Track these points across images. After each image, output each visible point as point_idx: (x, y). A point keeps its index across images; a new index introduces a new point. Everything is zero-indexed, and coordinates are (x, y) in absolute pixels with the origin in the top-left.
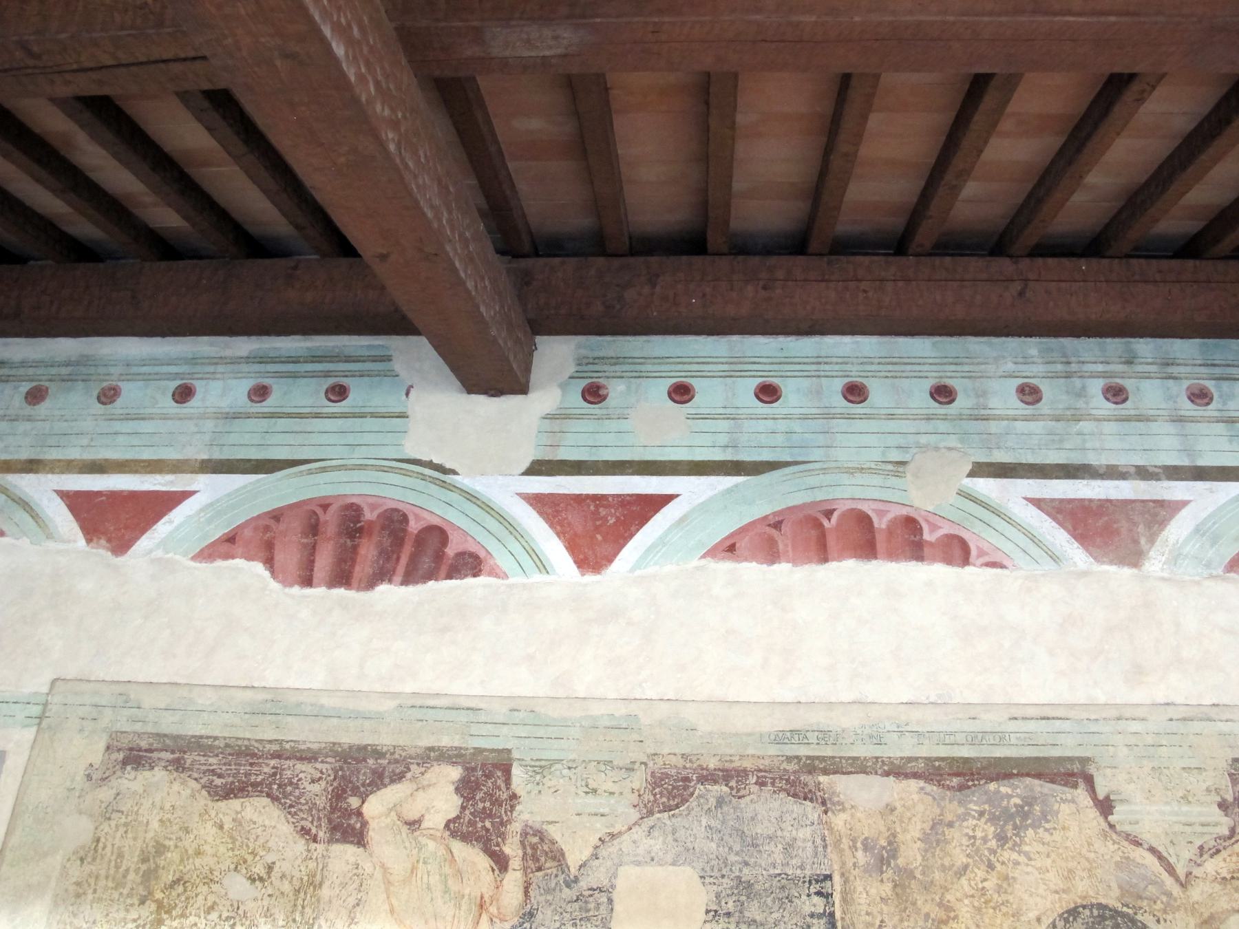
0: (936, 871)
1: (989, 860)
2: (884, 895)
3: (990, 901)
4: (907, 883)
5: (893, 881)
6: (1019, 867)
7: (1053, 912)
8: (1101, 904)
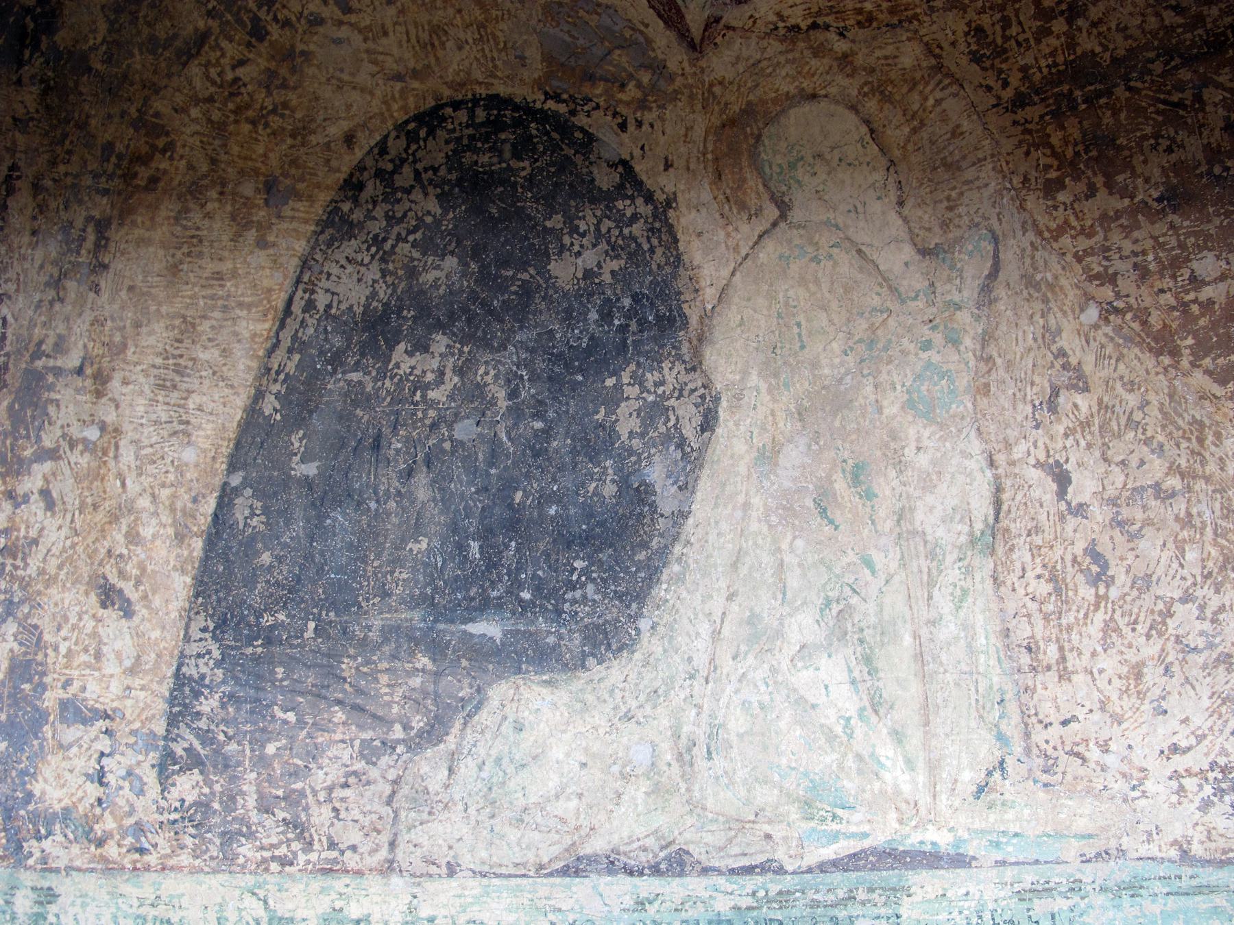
0: (136, 51)
1: (256, 19)
2: (20, 111)
3: (248, 107)
4: (71, 84)
5: (42, 81)
6: (321, 29)
7: (384, 121)
8: (497, 96)
